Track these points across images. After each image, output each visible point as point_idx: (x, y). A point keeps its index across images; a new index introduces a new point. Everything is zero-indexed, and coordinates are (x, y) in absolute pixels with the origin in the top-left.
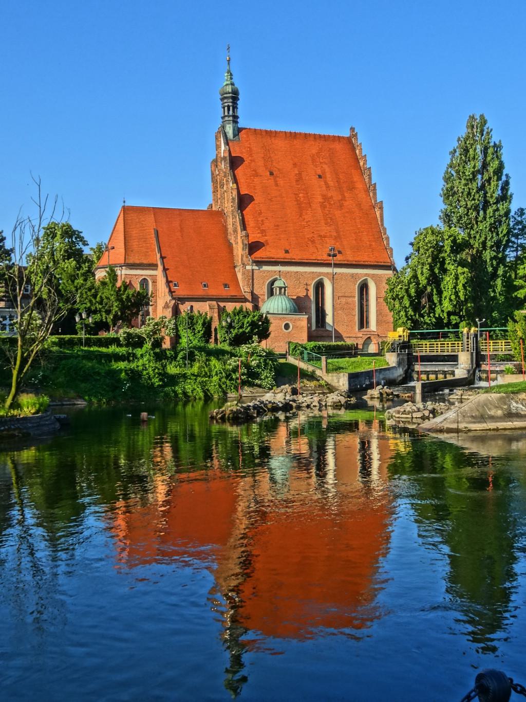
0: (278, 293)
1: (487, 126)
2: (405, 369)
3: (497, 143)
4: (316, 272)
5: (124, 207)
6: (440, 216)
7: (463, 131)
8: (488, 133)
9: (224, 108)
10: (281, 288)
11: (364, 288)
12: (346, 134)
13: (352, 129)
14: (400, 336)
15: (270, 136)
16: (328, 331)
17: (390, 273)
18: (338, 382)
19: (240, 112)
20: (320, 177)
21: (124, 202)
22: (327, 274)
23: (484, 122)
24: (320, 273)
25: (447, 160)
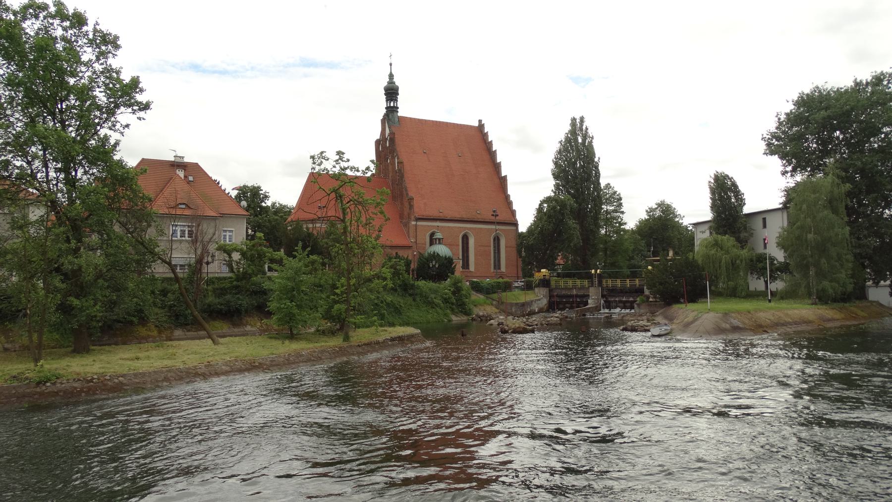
0: (437, 243)
5: (312, 174)
8: (587, 129)
9: (387, 101)
10: (439, 239)
11: (497, 240)
12: (476, 124)
13: (480, 121)
14: (544, 276)
17: (514, 228)
18: (511, 309)
19: (400, 104)
22: (470, 229)
23: (582, 120)
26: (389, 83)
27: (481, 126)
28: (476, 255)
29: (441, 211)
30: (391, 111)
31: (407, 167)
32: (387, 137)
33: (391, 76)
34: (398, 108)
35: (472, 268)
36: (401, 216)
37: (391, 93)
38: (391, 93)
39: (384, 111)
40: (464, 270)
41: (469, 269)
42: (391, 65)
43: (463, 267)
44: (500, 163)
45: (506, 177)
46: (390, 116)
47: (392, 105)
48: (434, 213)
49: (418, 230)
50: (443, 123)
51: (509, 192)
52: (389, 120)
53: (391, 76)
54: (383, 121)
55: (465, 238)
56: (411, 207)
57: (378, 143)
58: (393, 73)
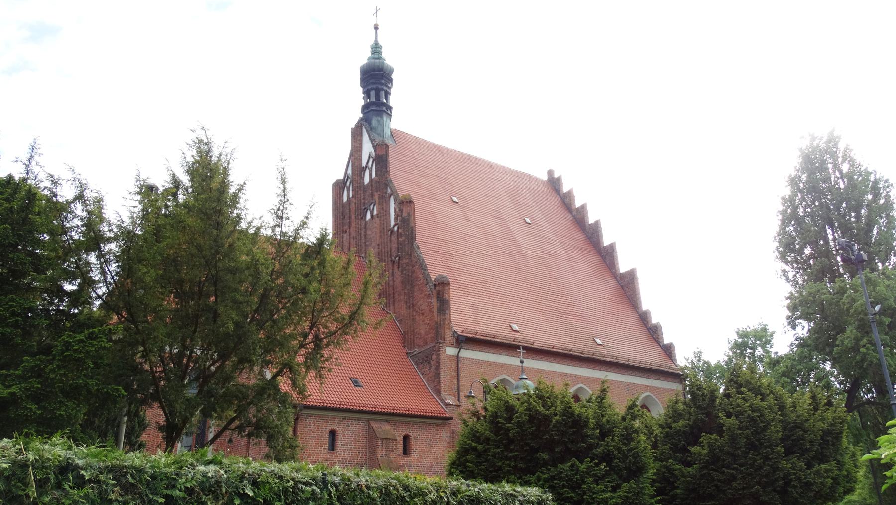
4: (571, 375)
24: (576, 376)
27: (554, 183)
29: (515, 327)
31: (421, 224)
32: (364, 164)
33: (376, 49)
36: (407, 339)
44: (612, 247)
46: (374, 122)
48: (501, 332)
49: (462, 374)
50: (483, 161)
51: (645, 307)
52: (371, 130)
53: (376, 49)
54: (357, 134)
56: (443, 305)
57: (339, 187)
58: (381, 42)
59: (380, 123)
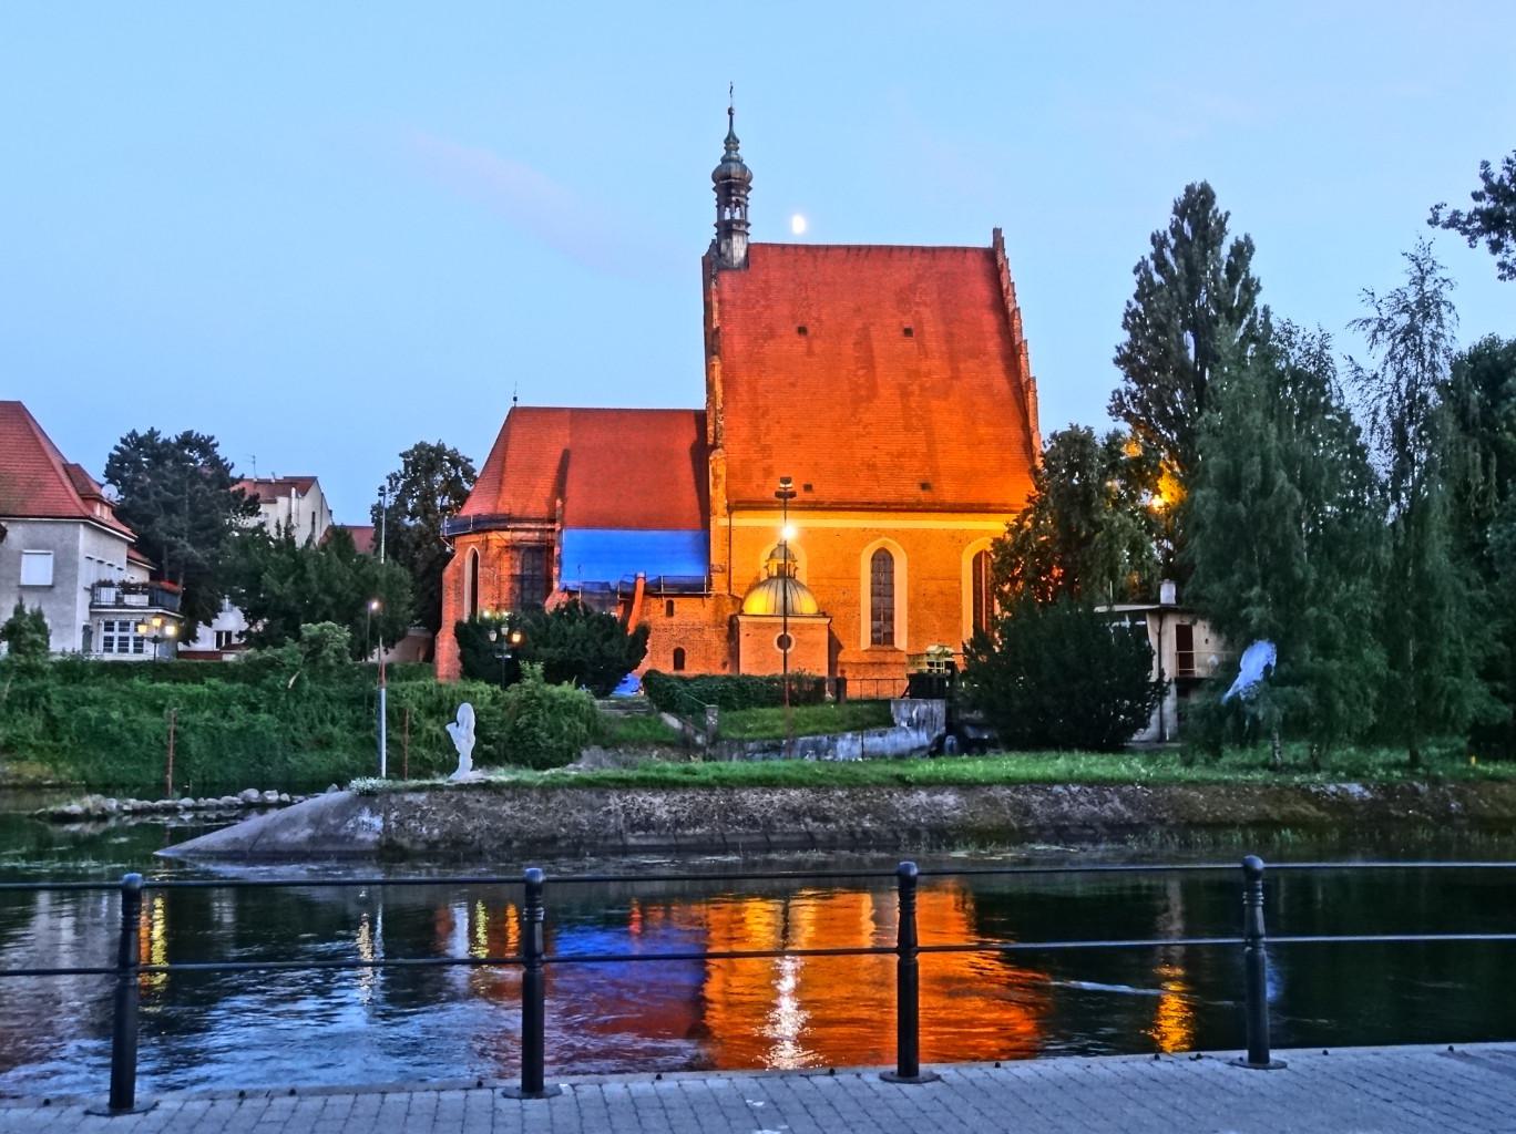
1: (1215, 207)
2: (936, 734)
3: (1242, 239)
4: (871, 530)
5: (514, 411)
6: (1110, 408)
7: (1163, 221)
9: (718, 206)
12: (987, 242)
13: (997, 232)
14: (931, 664)
15: (815, 257)
16: (896, 650)
20: (908, 332)
21: (515, 399)
22: (895, 534)
24: (877, 530)
25: (1131, 285)
26: (724, 160)
28: (912, 606)
30: (726, 230)
33: (731, 142)
34: (748, 225)
35: (901, 642)
37: (730, 185)
38: (730, 185)
39: (712, 233)
40: (876, 647)
41: (892, 643)
42: (730, 112)
43: (874, 641)
45: (1034, 379)
46: (723, 247)
47: (727, 216)
55: (883, 561)
59: (729, 246)
